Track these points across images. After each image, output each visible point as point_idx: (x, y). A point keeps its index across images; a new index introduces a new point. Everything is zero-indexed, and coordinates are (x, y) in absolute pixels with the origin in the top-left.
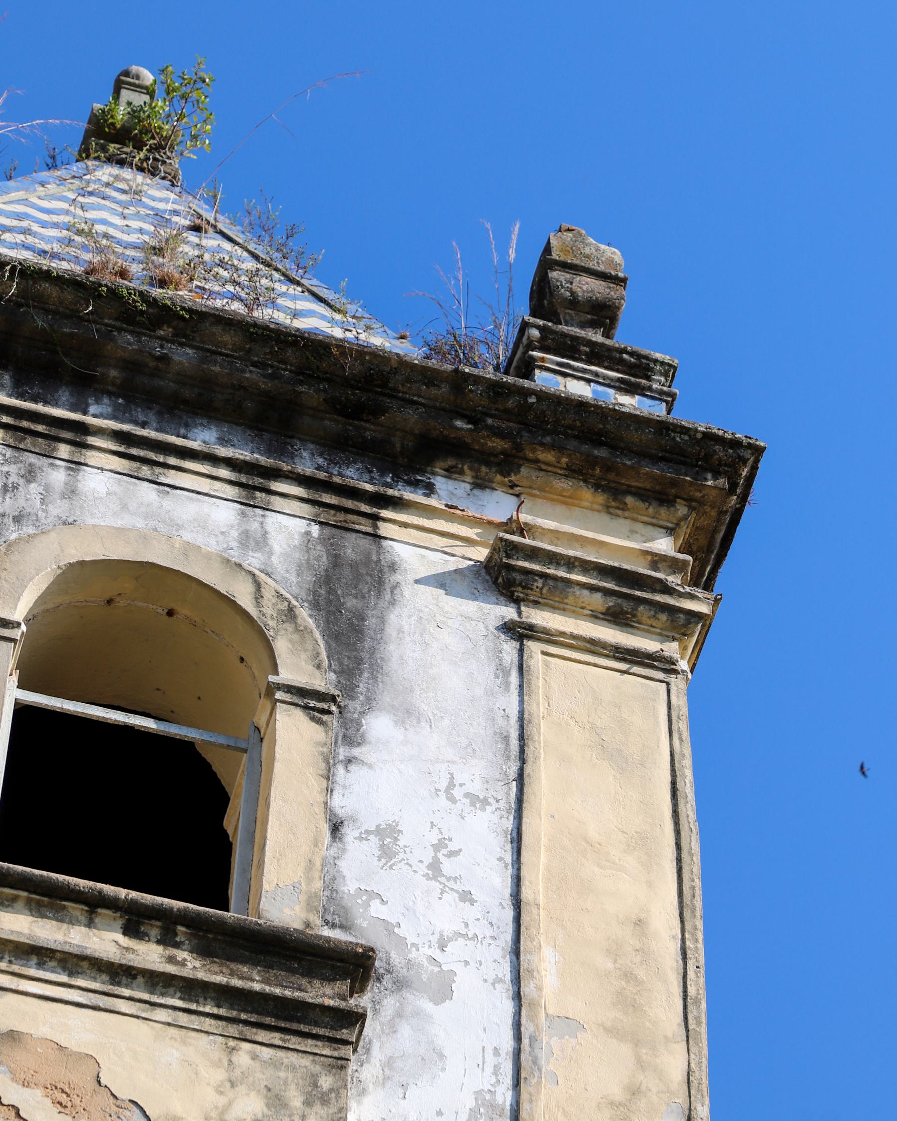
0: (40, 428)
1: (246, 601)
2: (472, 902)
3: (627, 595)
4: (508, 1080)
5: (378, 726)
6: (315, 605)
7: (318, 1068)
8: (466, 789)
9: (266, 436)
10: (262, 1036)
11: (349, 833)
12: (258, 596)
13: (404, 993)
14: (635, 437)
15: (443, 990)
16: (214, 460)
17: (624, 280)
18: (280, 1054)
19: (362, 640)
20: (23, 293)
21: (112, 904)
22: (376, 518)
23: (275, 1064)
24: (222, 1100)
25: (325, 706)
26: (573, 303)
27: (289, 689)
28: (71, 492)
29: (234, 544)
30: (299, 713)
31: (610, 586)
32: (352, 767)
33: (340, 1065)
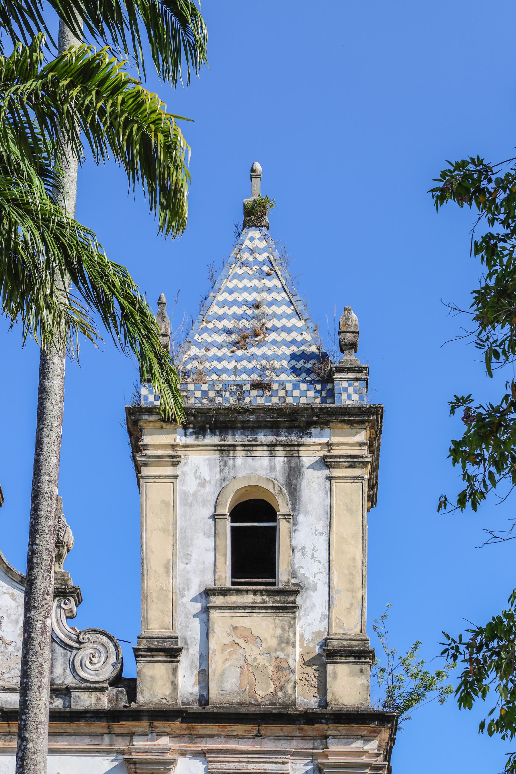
0: (226, 448)
1: (272, 491)
2: (320, 563)
3: (353, 462)
4: (327, 608)
5: (301, 518)
6: (286, 485)
7: (290, 619)
8: (319, 531)
9: (274, 430)
10: (280, 614)
11: (296, 551)
12: (274, 488)
13: (308, 592)
14: (353, 411)
15: (315, 589)
16: (262, 445)
17: (358, 332)
18: (284, 618)
19: (296, 493)
20: (216, 413)
21: (250, 591)
22: (298, 450)
23: (282, 620)
24: (274, 632)
25: (289, 517)
26: (346, 345)
27: (282, 515)
28: (234, 466)
29: (269, 471)
30: (284, 520)
31: (349, 460)
32: (296, 532)
33: (294, 618)
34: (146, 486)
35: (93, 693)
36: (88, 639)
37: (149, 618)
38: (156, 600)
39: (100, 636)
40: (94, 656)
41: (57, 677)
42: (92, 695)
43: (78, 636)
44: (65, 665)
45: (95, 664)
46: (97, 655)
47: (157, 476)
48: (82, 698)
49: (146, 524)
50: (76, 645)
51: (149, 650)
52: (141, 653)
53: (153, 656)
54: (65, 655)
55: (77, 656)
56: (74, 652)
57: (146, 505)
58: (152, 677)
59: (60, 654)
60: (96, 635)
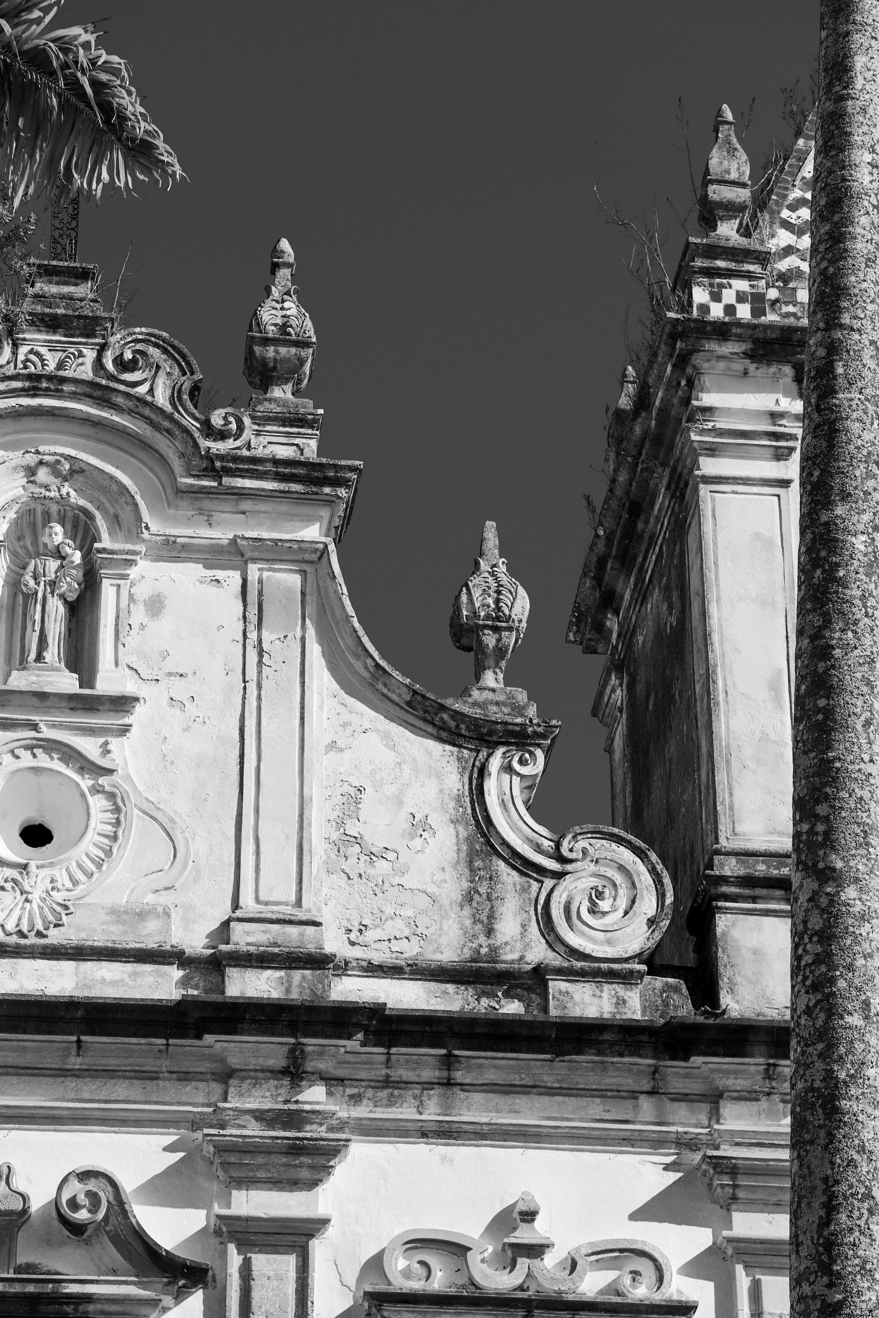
34: (713, 500)
35: (606, 987)
36: (584, 851)
37: (736, 806)
38: (752, 765)
39: (614, 845)
40: (600, 895)
41: (506, 943)
42: (602, 991)
43: (558, 845)
44: (526, 915)
45: (604, 914)
46: (607, 892)
47: (741, 478)
48: (577, 997)
49: (718, 586)
50: (552, 865)
51: (748, 881)
52: (725, 889)
53: (754, 899)
54: (525, 890)
55: (556, 894)
56: (549, 883)
57: (715, 543)
58: (755, 952)
59: (510, 887)
60: (604, 842)
